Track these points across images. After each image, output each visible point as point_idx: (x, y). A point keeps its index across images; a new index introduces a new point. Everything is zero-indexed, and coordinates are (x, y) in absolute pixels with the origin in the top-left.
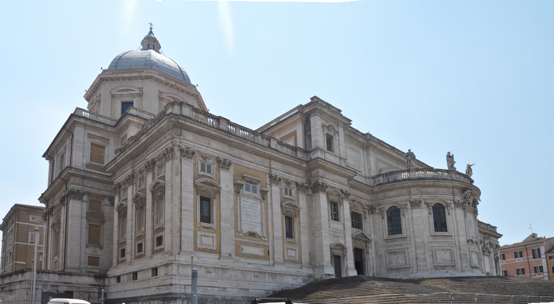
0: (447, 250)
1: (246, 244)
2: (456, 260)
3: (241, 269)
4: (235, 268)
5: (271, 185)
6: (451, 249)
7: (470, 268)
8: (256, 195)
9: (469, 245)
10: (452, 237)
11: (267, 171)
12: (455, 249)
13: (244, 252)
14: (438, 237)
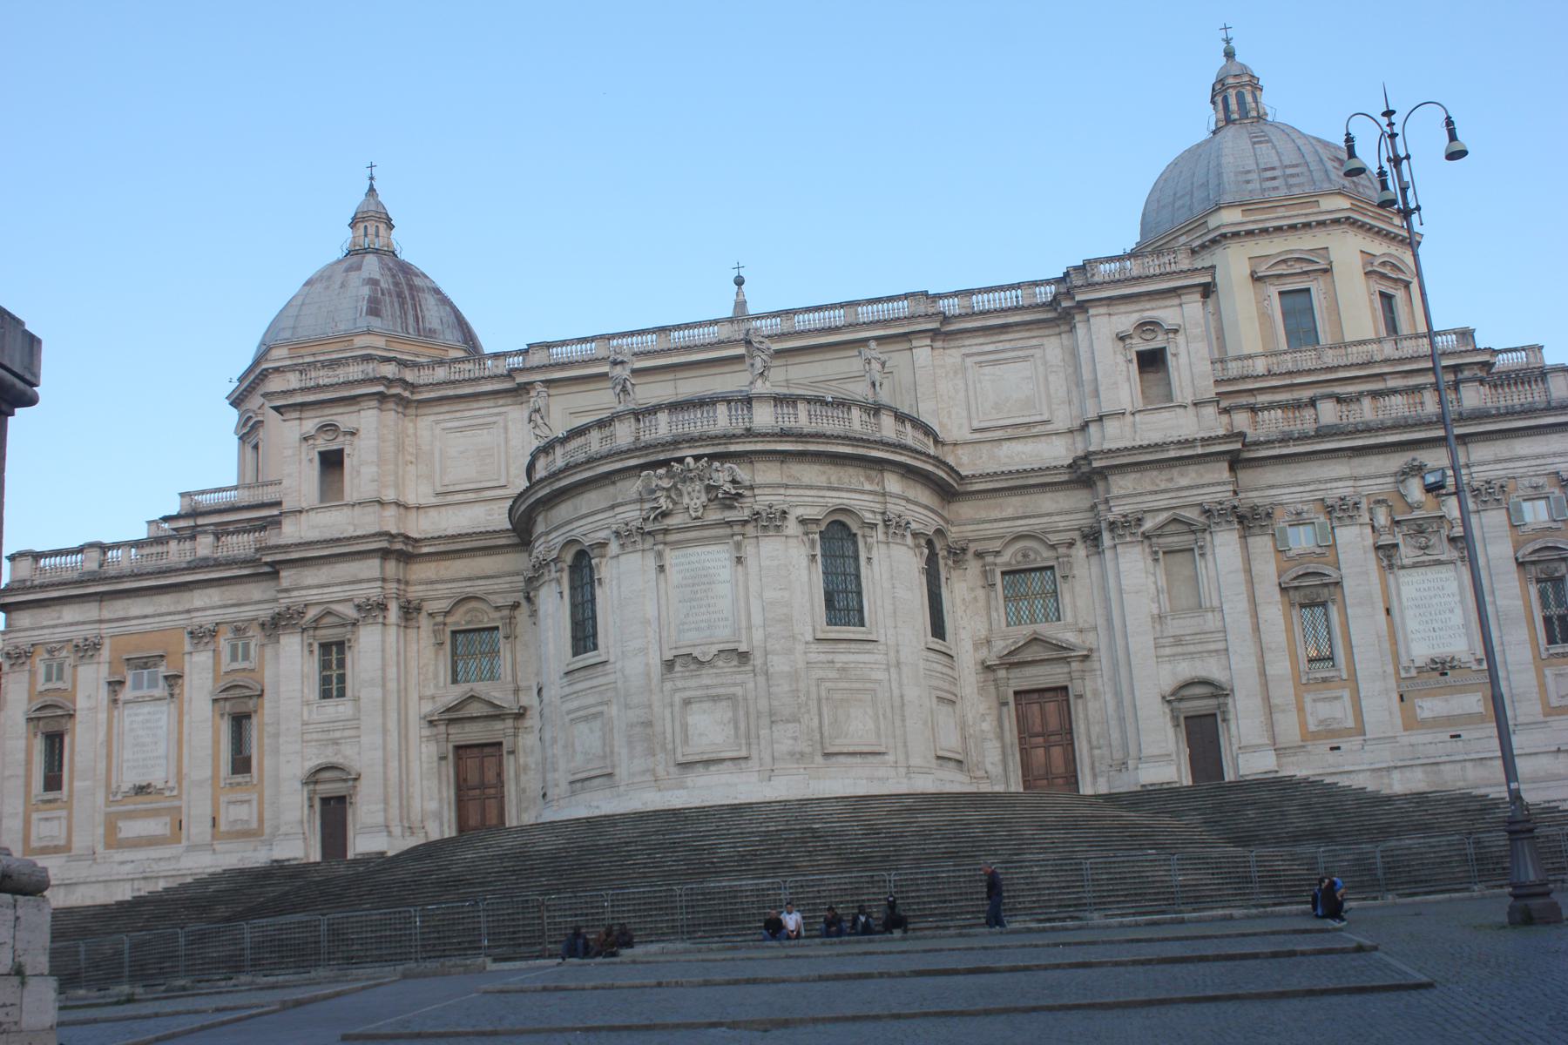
0: (595, 716)
1: (130, 815)
2: (616, 749)
3: (100, 879)
4: (88, 880)
5: (191, 653)
6: (602, 713)
7: (673, 770)
8: (157, 692)
9: (672, 680)
10: (608, 667)
11: (186, 622)
12: (614, 710)
13: (122, 835)
14: (576, 675)
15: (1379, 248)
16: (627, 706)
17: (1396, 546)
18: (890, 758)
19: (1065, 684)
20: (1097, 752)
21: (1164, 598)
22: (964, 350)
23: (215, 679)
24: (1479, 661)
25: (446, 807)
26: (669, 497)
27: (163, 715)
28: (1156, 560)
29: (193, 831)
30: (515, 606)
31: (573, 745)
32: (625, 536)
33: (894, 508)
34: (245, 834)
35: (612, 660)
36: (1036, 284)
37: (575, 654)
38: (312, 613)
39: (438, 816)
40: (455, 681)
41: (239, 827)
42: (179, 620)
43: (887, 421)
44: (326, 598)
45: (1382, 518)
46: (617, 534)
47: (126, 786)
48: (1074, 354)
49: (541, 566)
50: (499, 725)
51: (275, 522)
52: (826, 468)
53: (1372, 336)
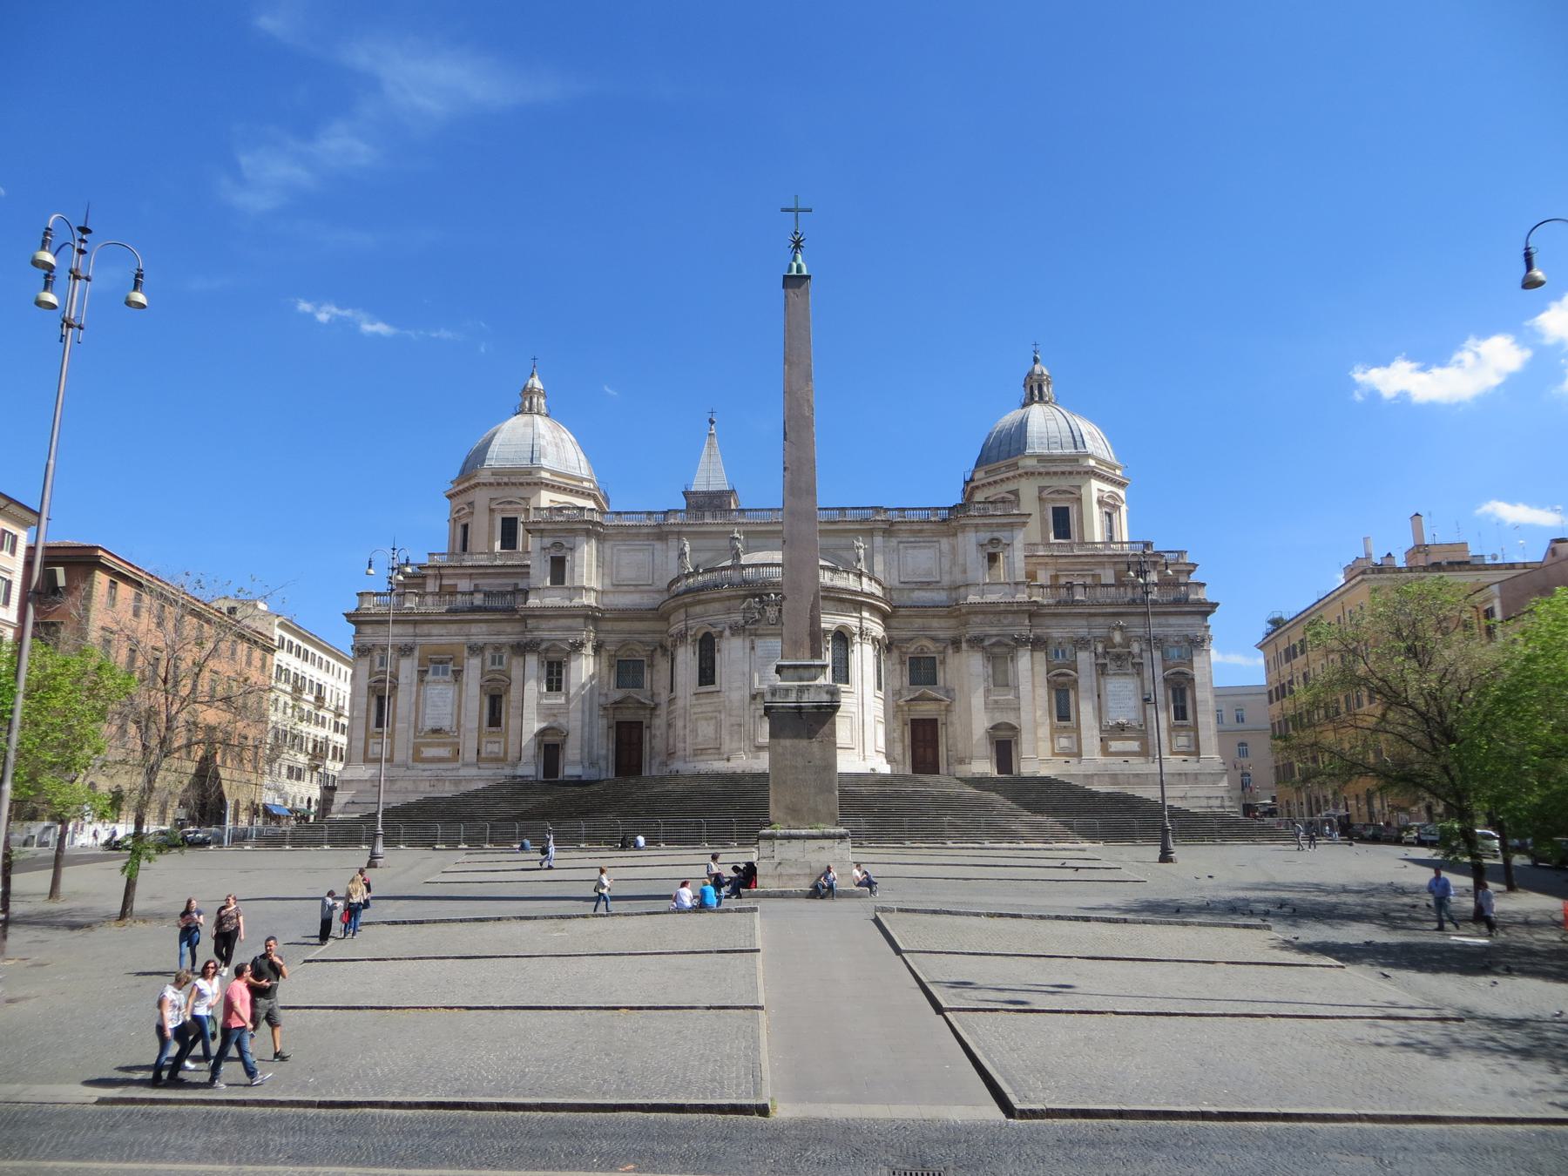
0: (711, 718)
6: (716, 718)
8: (447, 678)
10: (721, 694)
12: (723, 717)
13: (423, 755)
15: (1107, 488)
16: (730, 715)
17: (1106, 664)
18: (857, 751)
19: (935, 717)
20: (950, 753)
21: (991, 680)
22: (899, 539)
23: (482, 674)
24: (1141, 725)
25: (610, 753)
26: (759, 612)
27: (450, 692)
28: (989, 661)
29: (466, 756)
30: (656, 649)
31: (697, 731)
32: (736, 630)
33: (866, 624)
34: (496, 760)
35: (723, 690)
36: (938, 509)
37: (700, 685)
38: (544, 646)
39: (606, 758)
40: (618, 687)
41: (493, 755)
42: (462, 639)
43: (865, 580)
44: (553, 637)
45: (1100, 649)
46: (731, 628)
47: (427, 728)
48: (953, 549)
49: (682, 637)
50: (642, 712)
51: (526, 593)
52: (836, 603)
53: (1098, 538)
